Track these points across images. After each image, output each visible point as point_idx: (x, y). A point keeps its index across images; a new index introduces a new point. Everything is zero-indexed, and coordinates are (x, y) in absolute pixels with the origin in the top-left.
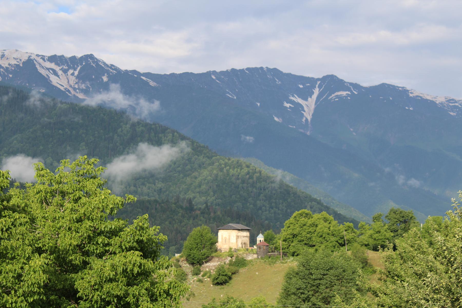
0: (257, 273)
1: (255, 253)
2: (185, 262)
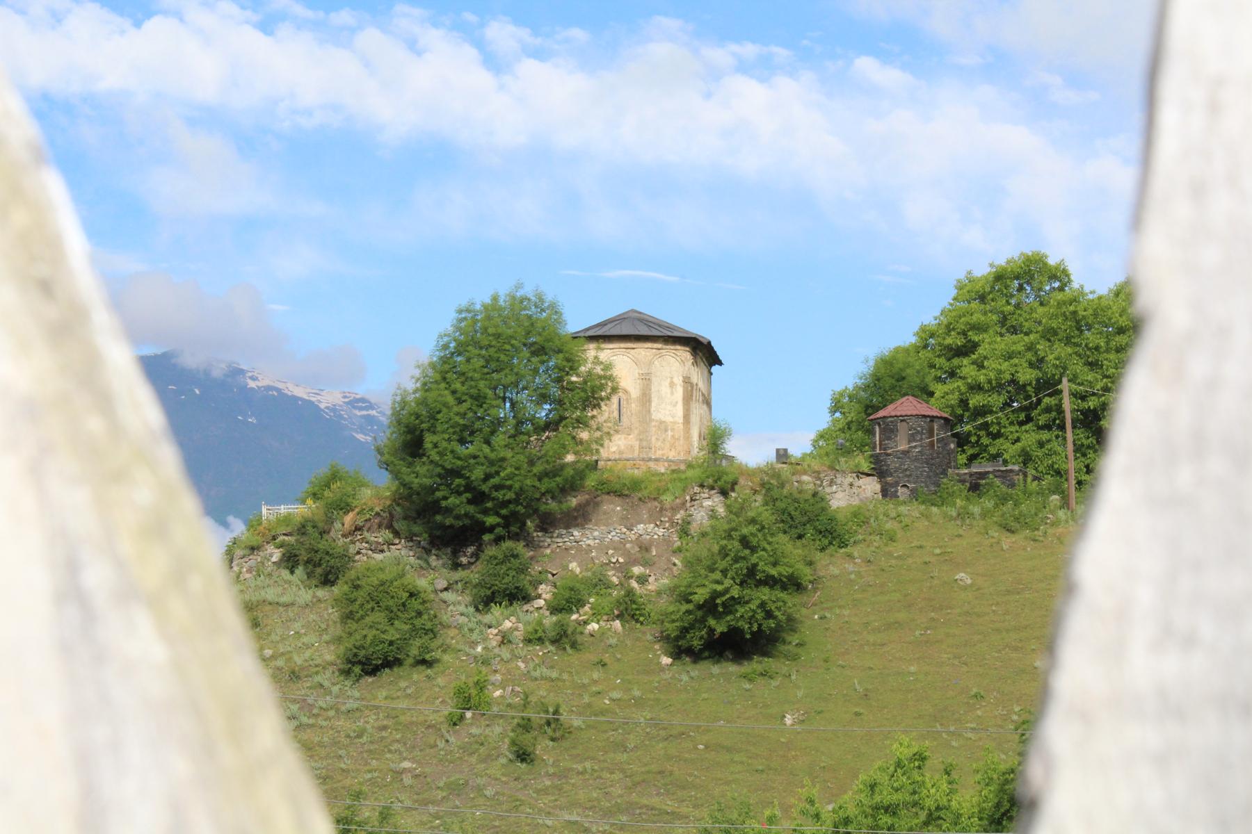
0: (964, 577)
1: (865, 467)
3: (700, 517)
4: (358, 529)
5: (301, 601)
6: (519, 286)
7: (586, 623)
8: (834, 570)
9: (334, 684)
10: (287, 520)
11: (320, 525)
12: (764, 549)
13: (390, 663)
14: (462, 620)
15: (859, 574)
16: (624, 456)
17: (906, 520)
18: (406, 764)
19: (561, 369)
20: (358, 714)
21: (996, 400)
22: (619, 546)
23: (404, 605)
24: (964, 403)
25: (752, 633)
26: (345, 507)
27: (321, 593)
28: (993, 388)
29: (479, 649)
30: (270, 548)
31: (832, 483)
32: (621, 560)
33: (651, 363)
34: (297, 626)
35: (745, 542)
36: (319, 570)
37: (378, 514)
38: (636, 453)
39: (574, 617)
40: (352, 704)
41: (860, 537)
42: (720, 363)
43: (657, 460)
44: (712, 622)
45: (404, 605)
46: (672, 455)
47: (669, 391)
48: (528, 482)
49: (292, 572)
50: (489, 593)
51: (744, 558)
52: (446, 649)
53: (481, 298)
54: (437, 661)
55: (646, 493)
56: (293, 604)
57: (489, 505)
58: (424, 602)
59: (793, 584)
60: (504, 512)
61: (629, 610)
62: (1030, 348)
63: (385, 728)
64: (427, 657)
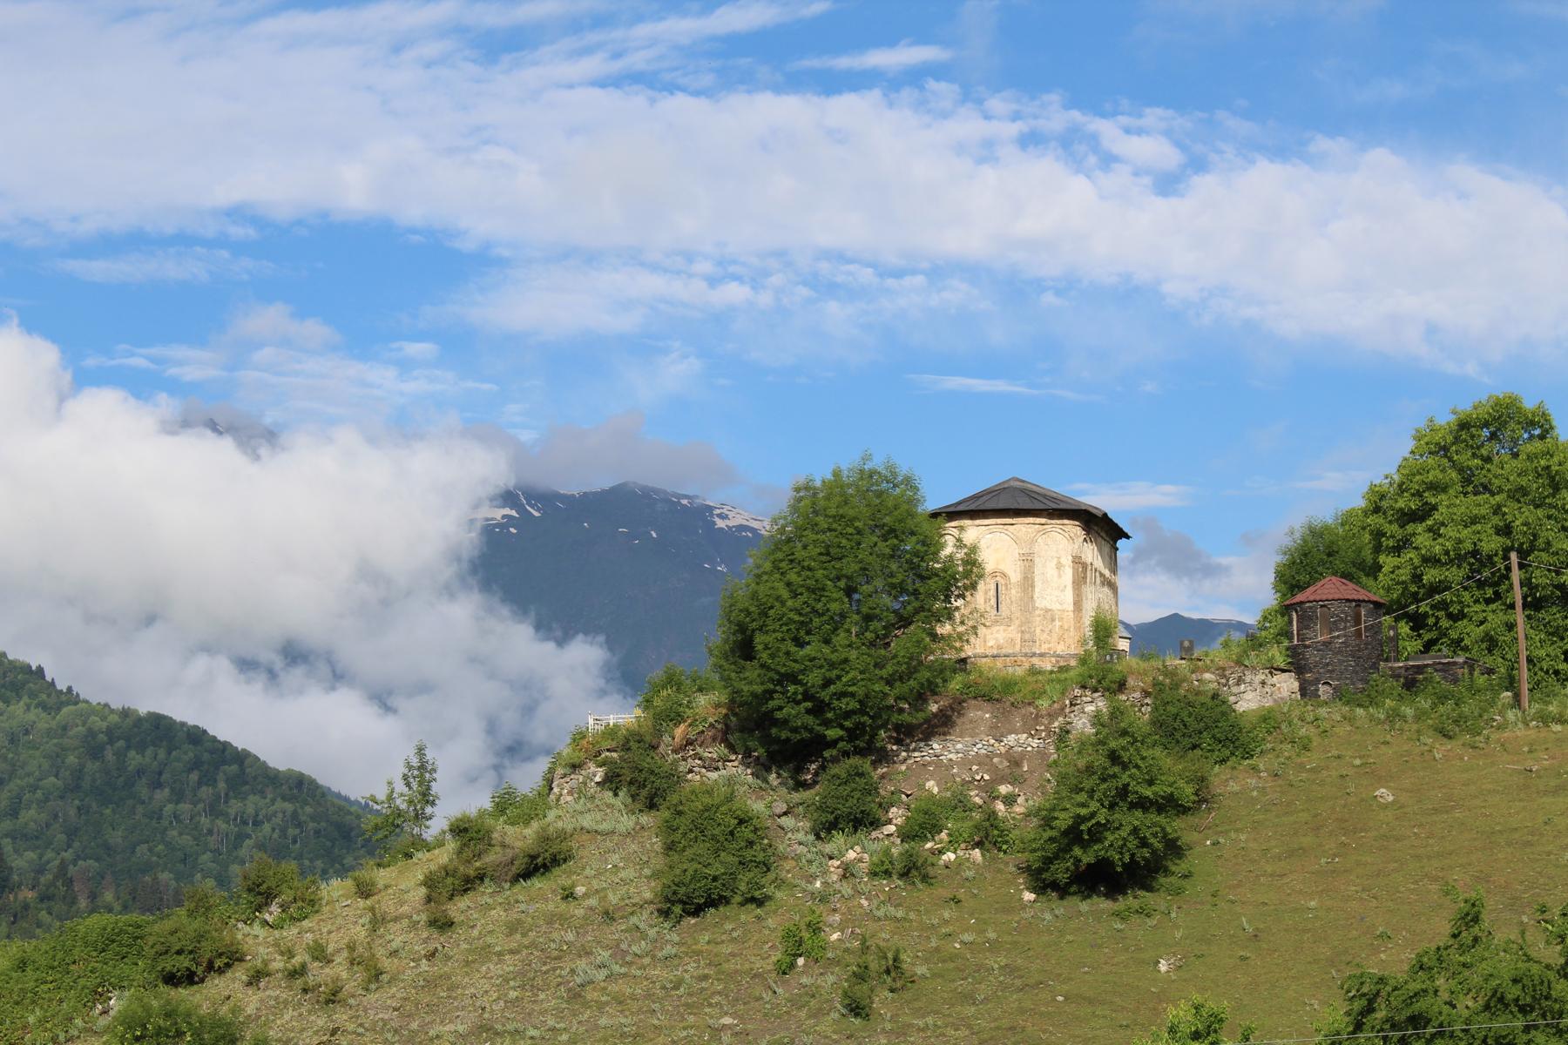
0: (1385, 794)
1: (1280, 661)
2: (714, 751)
3: (1082, 725)
4: (690, 743)
5: (622, 828)
6: (867, 458)
7: (941, 852)
8: (1234, 786)
9: (651, 926)
10: (611, 732)
11: (648, 738)
12: (1137, 767)
13: (713, 902)
14: (801, 849)
15: (1263, 791)
16: (1004, 651)
17: (1326, 725)
18: (727, 1020)
19: (916, 554)
20: (676, 962)
21: (1454, 574)
22: (985, 761)
23: (732, 833)
24: (1417, 578)
25: (1124, 864)
26: (678, 718)
27: (645, 819)
28: (1451, 561)
29: (818, 884)
30: (592, 767)
31: (1239, 681)
32: (987, 777)
33: (1033, 541)
34: (615, 858)
35: (1114, 757)
36: (644, 793)
37: (711, 725)
38: (1018, 648)
39: (929, 845)
40: (669, 950)
41: (1269, 746)
42: (1128, 537)
43: (1041, 655)
44: (1077, 851)
45: (732, 833)
46: (1061, 649)
47: (1055, 572)
48: (877, 687)
49: (616, 795)
50: (831, 818)
51: (1114, 776)
52: (780, 883)
53: (820, 474)
54: (768, 898)
55: (1019, 696)
56: (613, 832)
57: (830, 715)
58: (756, 830)
59: (1170, 805)
60: (847, 724)
61: (989, 835)
62: (1497, 510)
63: (705, 977)
64: (757, 894)
